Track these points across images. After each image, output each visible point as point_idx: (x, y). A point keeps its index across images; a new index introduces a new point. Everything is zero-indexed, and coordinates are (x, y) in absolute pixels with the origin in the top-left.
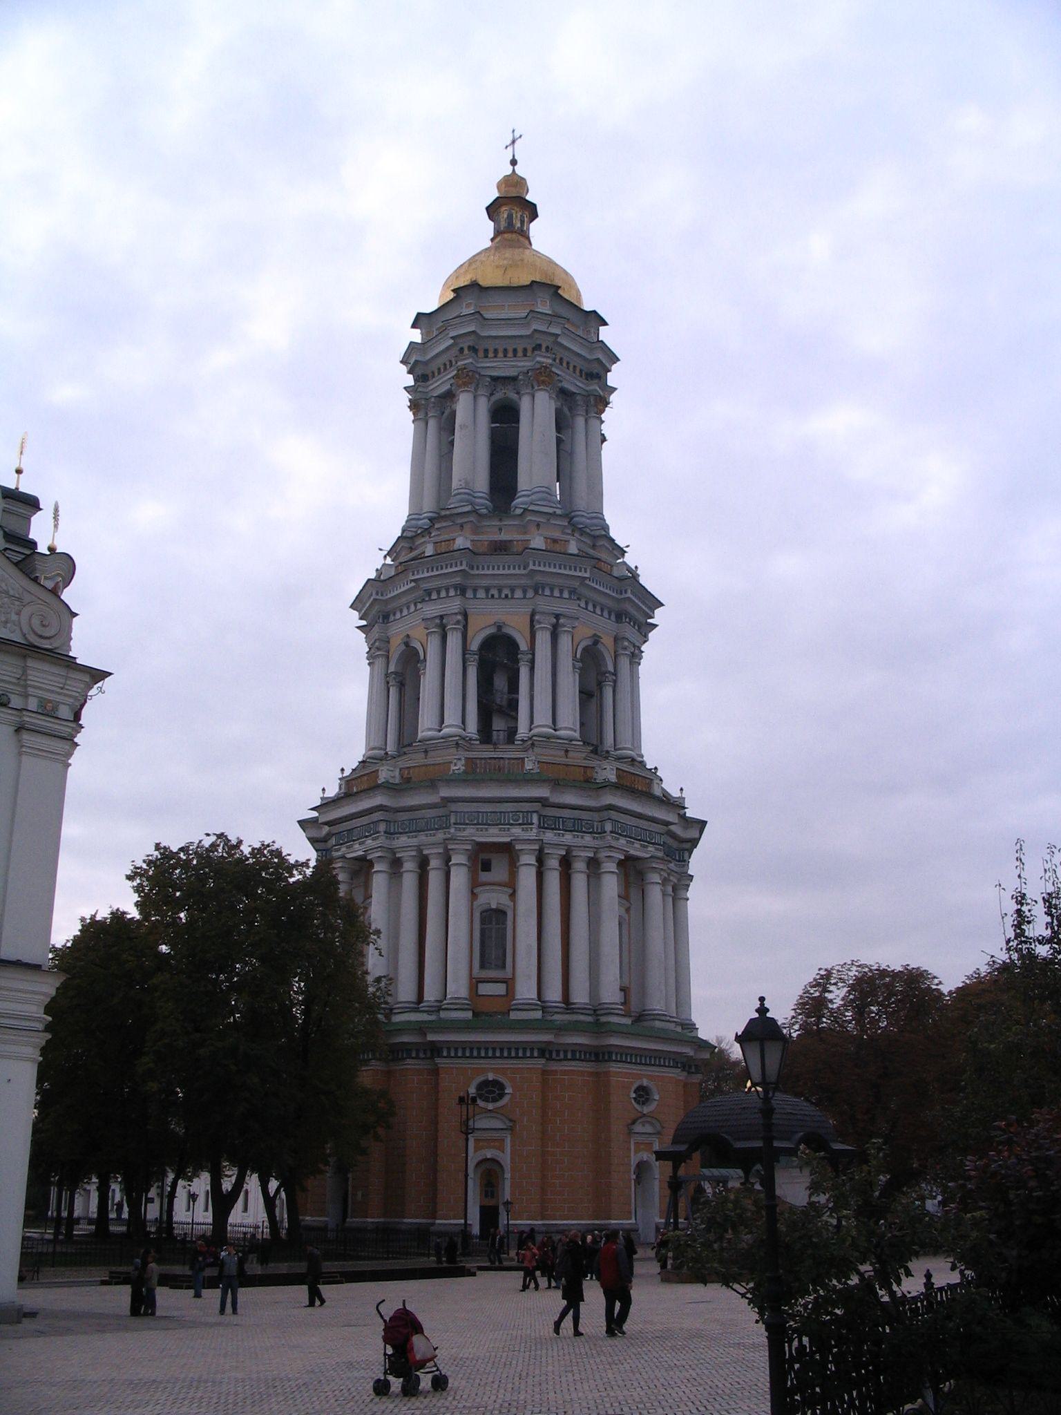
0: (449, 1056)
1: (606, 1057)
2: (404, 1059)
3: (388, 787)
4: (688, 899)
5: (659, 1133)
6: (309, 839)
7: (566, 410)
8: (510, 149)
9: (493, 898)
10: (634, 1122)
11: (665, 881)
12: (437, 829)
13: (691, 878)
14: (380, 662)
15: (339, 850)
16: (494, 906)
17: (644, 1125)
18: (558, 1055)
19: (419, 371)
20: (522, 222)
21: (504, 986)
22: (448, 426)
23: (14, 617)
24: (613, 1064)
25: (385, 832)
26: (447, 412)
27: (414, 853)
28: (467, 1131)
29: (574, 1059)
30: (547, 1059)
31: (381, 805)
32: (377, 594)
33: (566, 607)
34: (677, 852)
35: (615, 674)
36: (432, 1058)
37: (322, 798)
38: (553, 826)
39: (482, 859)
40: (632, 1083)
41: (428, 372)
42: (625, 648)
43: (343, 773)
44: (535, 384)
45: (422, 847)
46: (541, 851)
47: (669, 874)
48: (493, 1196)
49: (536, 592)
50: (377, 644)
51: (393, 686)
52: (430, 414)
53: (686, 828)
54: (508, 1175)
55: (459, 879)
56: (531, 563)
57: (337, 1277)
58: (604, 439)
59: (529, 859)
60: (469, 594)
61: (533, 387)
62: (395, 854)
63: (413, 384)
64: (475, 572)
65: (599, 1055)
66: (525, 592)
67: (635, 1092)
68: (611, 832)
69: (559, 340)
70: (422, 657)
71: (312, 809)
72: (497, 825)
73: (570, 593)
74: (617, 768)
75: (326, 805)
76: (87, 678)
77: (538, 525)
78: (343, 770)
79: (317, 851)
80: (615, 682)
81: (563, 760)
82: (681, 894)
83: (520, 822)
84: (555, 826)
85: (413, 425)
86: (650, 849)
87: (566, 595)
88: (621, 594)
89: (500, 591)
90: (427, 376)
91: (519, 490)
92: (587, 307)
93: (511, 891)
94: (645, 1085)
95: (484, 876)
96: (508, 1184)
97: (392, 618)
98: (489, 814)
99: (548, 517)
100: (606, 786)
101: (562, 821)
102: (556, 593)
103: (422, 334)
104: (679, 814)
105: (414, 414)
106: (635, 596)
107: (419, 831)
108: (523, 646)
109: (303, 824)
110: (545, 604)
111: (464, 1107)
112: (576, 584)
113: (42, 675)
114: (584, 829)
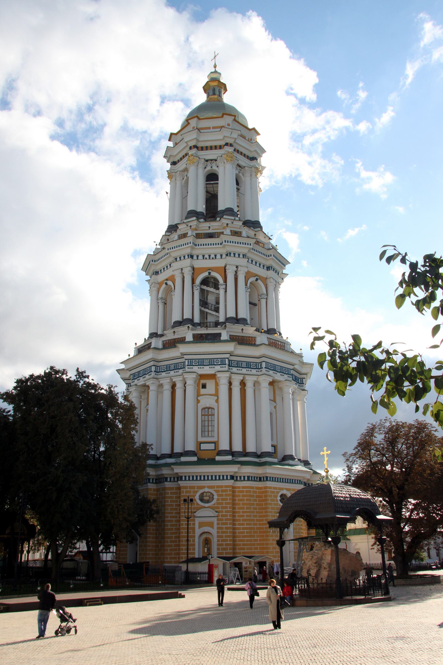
0: (185, 480)
1: (265, 479)
2: (163, 482)
6: (122, 378)
7: (241, 174)
8: (214, 61)
12: (179, 369)
14: (155, 293)
16: (208, 406)
19: (172, 160)
21: (214, 444)
24: (267, 482)
25: (155, 371)
26: (185, 178)
27: (169, 381)
29: (248, 480)
30: (235, 480)
33: (243, 262)
34: (300, 379)
35: (267, 295)
36: (178, 480)
38: (236, 366)
39: (202, 384)
40: (278, 493)
41: (176, 160)
43: (136, 345)
44: (225, 161)
45: (172, 378)
46: (230, 378)
49: (227, 255)
60: (195, 257)
61: (224, 163)
62: (159, 381)
64: (197, 247)
66: (221, 255)
68: (265, 368)
71: (121, 363)
73: (243, 255)
78: (136, 344)
79: (126, 384)
80: (267, 299)
83: (220, 363)
84: (237, 365)
85: (170, 185)
87: (241, 256)
89: (210, 256)
91: (219, 210)
92: (250, 127)
93: (216, 398)
95: (203, 391)
97: (160, 272)
98: (204, 360)
99: (232, 221)
101: (241, 363)
102: (237, 255)
103: (173, 144)
104: (299, 360)
108: (221, 281)
109: (118, 371)
114: (252, 367)
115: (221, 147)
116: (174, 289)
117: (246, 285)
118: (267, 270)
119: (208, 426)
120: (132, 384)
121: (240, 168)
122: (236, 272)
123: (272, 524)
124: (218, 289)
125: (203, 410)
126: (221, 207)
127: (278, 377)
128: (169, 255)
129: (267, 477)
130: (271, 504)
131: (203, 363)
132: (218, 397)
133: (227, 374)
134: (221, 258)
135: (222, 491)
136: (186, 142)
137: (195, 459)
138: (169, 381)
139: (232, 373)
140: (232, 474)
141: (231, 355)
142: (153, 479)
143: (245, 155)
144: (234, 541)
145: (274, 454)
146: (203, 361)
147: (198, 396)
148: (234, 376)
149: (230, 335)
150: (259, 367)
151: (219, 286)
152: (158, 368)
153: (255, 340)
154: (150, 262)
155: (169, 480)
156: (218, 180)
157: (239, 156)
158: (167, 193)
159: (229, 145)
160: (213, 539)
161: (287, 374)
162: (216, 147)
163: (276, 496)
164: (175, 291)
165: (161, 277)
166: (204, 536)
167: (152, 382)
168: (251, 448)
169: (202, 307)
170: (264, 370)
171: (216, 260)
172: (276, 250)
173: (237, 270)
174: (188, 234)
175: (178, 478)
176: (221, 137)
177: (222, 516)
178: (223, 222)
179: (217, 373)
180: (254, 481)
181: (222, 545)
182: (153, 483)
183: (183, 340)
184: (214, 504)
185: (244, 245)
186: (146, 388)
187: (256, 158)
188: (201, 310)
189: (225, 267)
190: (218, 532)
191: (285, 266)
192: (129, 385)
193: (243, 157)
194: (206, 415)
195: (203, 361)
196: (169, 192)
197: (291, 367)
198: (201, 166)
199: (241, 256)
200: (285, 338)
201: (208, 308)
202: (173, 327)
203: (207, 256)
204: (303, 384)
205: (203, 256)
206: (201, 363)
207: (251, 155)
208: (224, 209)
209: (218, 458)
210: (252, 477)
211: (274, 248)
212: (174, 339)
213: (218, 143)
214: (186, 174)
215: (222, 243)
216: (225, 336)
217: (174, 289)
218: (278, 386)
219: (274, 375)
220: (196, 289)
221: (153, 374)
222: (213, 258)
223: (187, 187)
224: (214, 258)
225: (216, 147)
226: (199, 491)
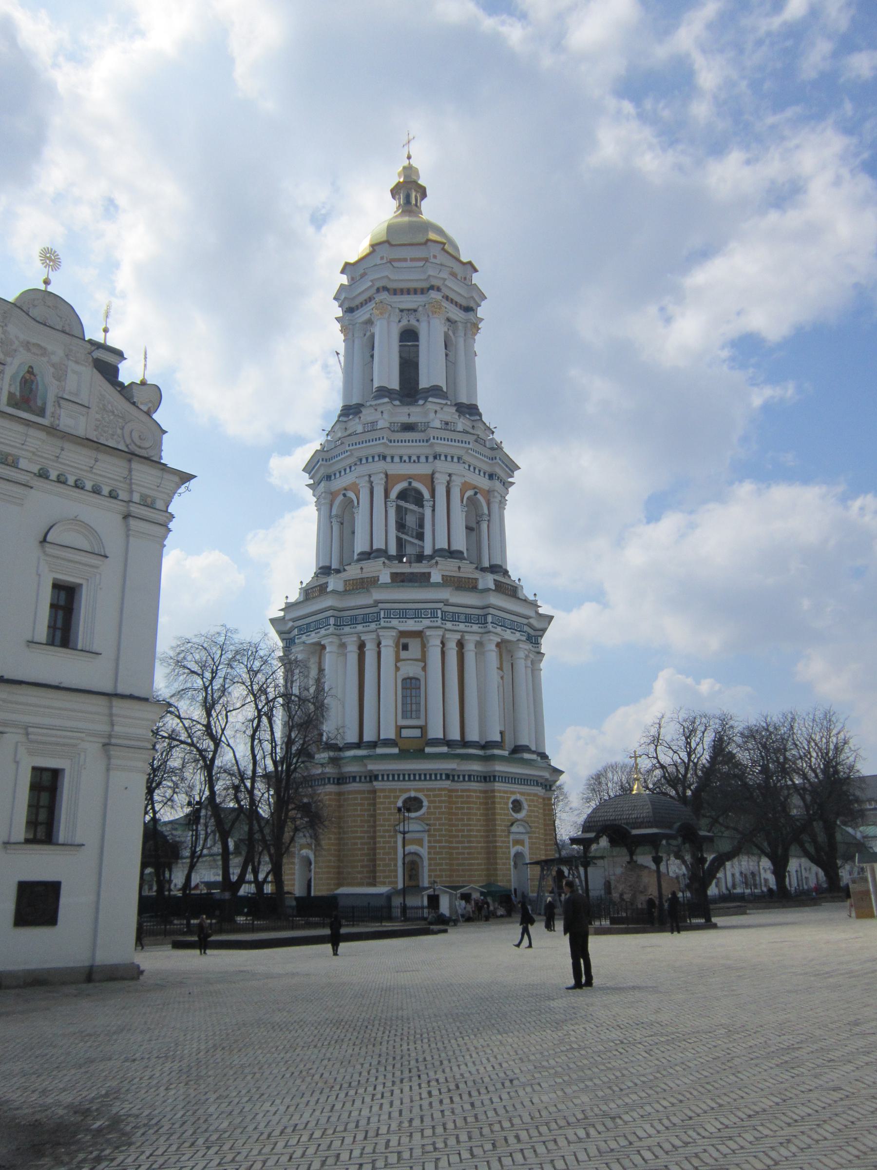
1: (492, 780)
2: (349, 783)
4: (541, 670)
5: (528, 833)
7: (450, 333)
8: (406, 148)
9: (410, 669)
10: (512, 825)
15: (301, 638)
16: (411, 675)
21: (420, 730)
23: (119, 431)
24: (496, 784)
25: (334, 625)
26: (368, 334)
29: (470, 780)
31: (331, 606)
35: (489, 515)
36: (371, 781)
37: (286, 603)
40: (508, 798)
41: (353, 305)
45: (361, 635)
46: (443, 637)
49: (435, 458)
50: (323, 495)
52: (356, 335)
54: (426, 863)
56: (432, 438)
58: (476, 355)
60: (389, 459)
61: (428, 316)
62: (341, 640)
63: (341, 315)
64: (393, 444)
65: (488, 778)
66: (427, 458)
67: (512, 803)
68: (492, 623)
69: (447, 283)
70: (356, 504)
73: (459, 458)
74: (494, 580)
75: (289, 607)
76: (176, 479)
77: (436, 412)
78: (301, 582)
80: (489, 521)
83: (429, 616)
87: (455, 460)
89: (410, 458)
91: (420, 387)
92: (464, 259)
93: (423, 664)
94: (518, 798)
95: (404, 654)
97: (333, 477)
99: (442, 406)
100: (488, 590)
102: (449, 459)
105: (344, 336)
108: (427, 495)
109: (273, 621)
110: (440, 465)
113: (143, 475)
115: (423, 291)
116: (358, 503)
117: (462, 502)
118: (489, 479)
119: (411, 704)
120: (297, 641)
121: (450, 323)
122: (448, 483)
124: (422, 506)
126: (424, 383)
127: (508, 635)
128: (349, 453)
129: (494, 777)
130: (501, 814)
132: (425, 665)
133: (440, 632)
134: (427, 461)
135: (435, 796)
136: (372, 281)
137: (396, 750)
138: (355, 639)
139: (446, 630)
142: (334, 779)
143: (456, 304)
147: (396, 663)
148: (448, 635)
149: (442, 575)
151: (424, 503)
153: (476, 582)
154: (318, 461)
155: (358, 779)
158: (338, 354)
159: (435, 288)
160: (423, 861)
161: (519, 631)
162: (415, 291)
163: (507, 803)
165: (338, 484)
167: (330, 640)
168: (473, 735)
169: (399, 531)
171: (419, 464)
172: (501, 449)
173: (450, 480)
174: (379, 423)
175: (370, 777)
177: (435, 830)
180: (477, 781)
181: (435, 870)
182: (334, 783)
183: (374, 580)
184: (424, 814)
185: (460, 444)
187: (472, 308)
189: (433, 474)
190: (429, 853)
191: (513, 472)
193: (454, 306)
196: (342, 351)
197: (525, 621)
198: (395, 319)
199: (455, 460)
201: (406, 534)
202: (359, 560)
203: (406, 458)
205: (401, 458)
207: (464, 303)
208: (427, 386)
209: (428, 750)
212: (362, 578)
215: (430, 439)
216: (436, 577)
217: (358, 503)
219: (503, 633)
221: (332, 629)
222: (414, 461)
223: (373, 349)
225: (415, 291)
226: (400, 796)
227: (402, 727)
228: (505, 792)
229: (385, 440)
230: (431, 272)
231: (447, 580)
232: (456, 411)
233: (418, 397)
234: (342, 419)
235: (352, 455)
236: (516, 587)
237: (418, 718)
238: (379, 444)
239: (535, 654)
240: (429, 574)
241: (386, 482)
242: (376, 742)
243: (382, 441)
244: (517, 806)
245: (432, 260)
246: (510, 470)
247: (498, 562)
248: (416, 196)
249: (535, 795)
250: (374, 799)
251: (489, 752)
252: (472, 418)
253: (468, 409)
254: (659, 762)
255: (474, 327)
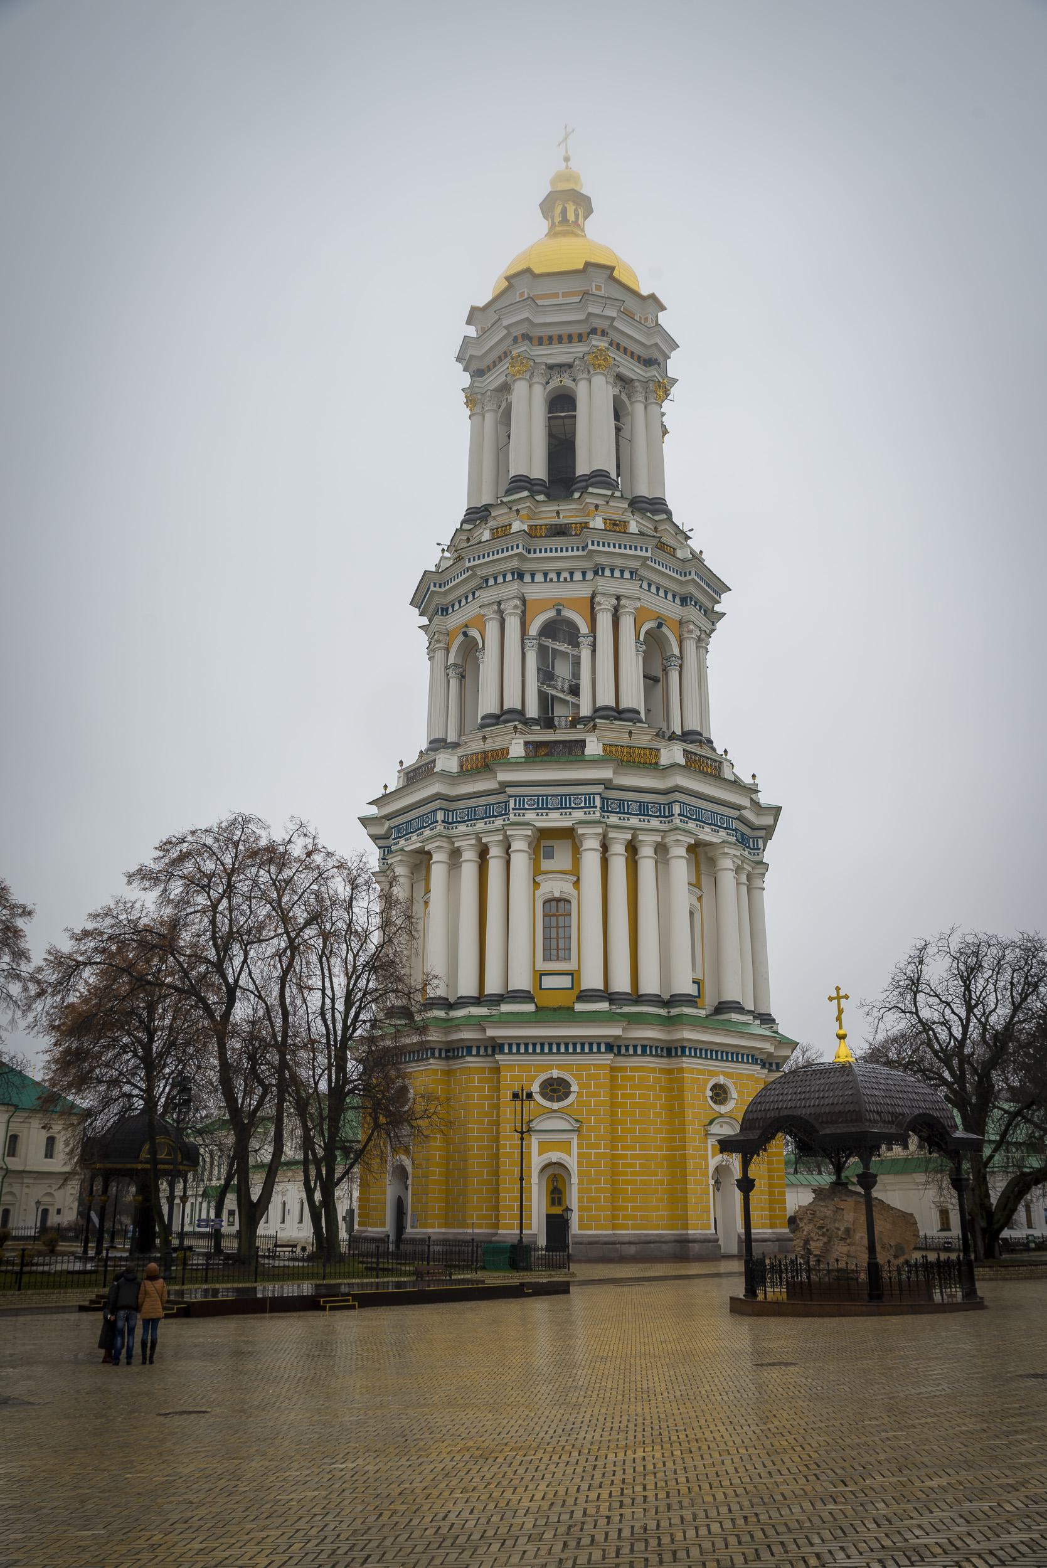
1: (679, 1053)
2: (463, 1056)
3: (445, 775)
6: (371, 836)
7: (624, 397)
10: (711, 1123)
11: (738, 870)
12: (496, 816)
13: (766, 866)
14: (440, 655)
15: (397, 843)
16: (557, 895)
17: (721, 1126)
18: (627, 1049)
19: (475, 366)
20: (577, 216)
22: (506, 418)
24: (685, 1059)
25: (443, 822)
26: (504, 405)
27: (473, 842)
28: (524, 1132)
29: (644, 1053)
31: (437, 794)
32: (435, 586)
33: (628, 588)
34: (751, 840)
35: (681, 658)
36: (493, 1055)
41: (483, 366)
42: (691, 632)
43: (401, 766)
45: (480, 835)
47: (742, 862)
48: (560, 1204)
49: (596, 573)
51: (452, 677)
52: (486, 408)
53: (758, 814)
54: (575, 1180)
55: (520, 863)
57: (348, 1301)
58: (665, 432)
59: (591, 844)
60: (527, 578)
61: (589, 372)
62: (453, 843)
64: (532, 555)
65: (671, 1050)
66: (584, 574)
68: (679, 815)
70: (481, 646)
72: (558, 809)
73: (631, 573)
78: (401, 763)
79: (379, 848)
80: (681, 666)
81: (628, 743)
82: (757, 883)
83: (583, 805)
86: (720, 833)
87: (627, 575)
88: (685, 576)
89: (559, 575)
90: (483, 370)
92: (645, 292)
95: (546, 865)
96: (575, 1190)
97: (450, 610)
102: (617, 574)
106: (702, 579)
107: (477, 819)
108: (584, 629)
109: (364, 821)
110: (607, 585)
111: (518, 1103)
112: (637, 564)
115: (580, 338)
118: (682, 605)
119: (558, 938)
121: (623, 384)
122: (616, 609)
123: (726, 1146)
124: (577, 645)
125: (547, 905)
126: (583, 468)
128: (470, 572)
129: (683, 1048)
131: (547, 805)
132: (578, 879)
135: (589, 1076)
136: (506, 327)
137: (531, 1008)
138: (473, 842)
140: (610, 1041)
141: (606, 788)
142: (440, 1050)
144: (614, 1182)
145: (697, 999)
146: (547, 799)
150: (667, 814)
152: (450, 813)
155: (474, 1052)
156: (575, 410)
157: (619, 357)
159: (599, 332)
161: (725, 828)
162: (570, 338)
164: (486, 650)
165: (455, 620)
166: (550, 1171)
167: (437, 844)
168: (650, 985)
169: (542, 684)
170: (677, 821)
172: (701, 561)
173: (619, 603)
174: (513, 526)
175: (494, 1048)
176: (582, 317)
178: (588, 500)
179: (576, 826)
180: (657, 1055)
182: (440, 1057)
186: (427, 857)
187: (656, 360)
188: (539, 691)
190: (580, 1164)
192: (386, 852)
194: (553, 915)
195: (547, 799)
197: (735, 814)
200: (720, 751)
202: (483, 726)
204: (759, 849)
205: (545, 575)
206: (543, 805)
209: (579, 1007)
210: (651, 1047)
211: (697, 558)
213: (575, 330)
214: (505, 397)
215: (587, 546)
216: (593, 747)
218: (706, 853)
219: (697, 831)
220: (531, 645)
221: (440, 828)
223: (509, 425)
224: (569, 579)
225: (570, 338)
227: (543, 974)
228: (700, 1072)
229: (520, 550)
230: (592, 309)
231: (611, 751)
232: (629, 505)
233: (574, 487)
234: (466, 527)
235: (474, 575)
236: (721, 762)
237: (567, 959)
238: (512, 556)
239: (753, 865)
240: (584, 741)
241: (524, 612)
242: (502, 995)
243: (516, 551)
244: (720, 1094)
245: (594, 291)
246: (715, 591)
247: (692, 725)
248: (576, 210)
249: (749, 1077)
250: (499, 1082)
251: (675, 1011)
252: (657, 518)
253: (650, 504)
254: (920, 1021)
255: (662, 388)
